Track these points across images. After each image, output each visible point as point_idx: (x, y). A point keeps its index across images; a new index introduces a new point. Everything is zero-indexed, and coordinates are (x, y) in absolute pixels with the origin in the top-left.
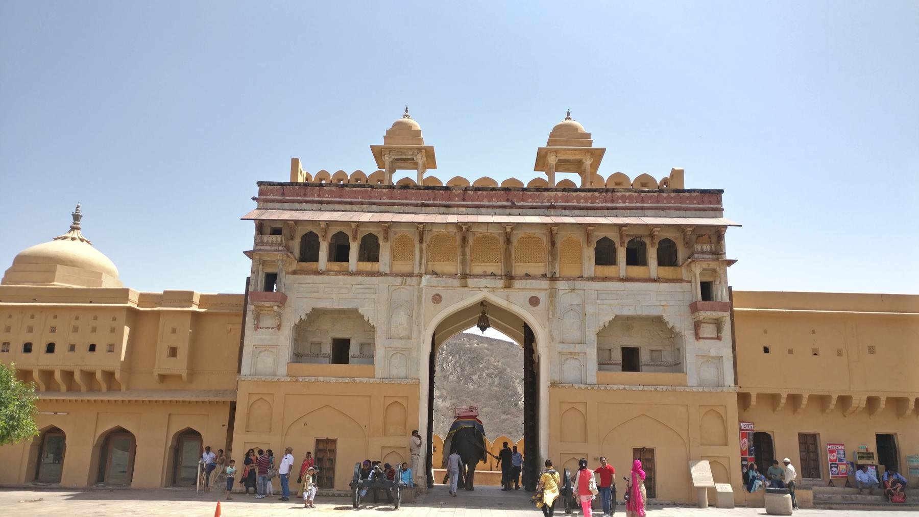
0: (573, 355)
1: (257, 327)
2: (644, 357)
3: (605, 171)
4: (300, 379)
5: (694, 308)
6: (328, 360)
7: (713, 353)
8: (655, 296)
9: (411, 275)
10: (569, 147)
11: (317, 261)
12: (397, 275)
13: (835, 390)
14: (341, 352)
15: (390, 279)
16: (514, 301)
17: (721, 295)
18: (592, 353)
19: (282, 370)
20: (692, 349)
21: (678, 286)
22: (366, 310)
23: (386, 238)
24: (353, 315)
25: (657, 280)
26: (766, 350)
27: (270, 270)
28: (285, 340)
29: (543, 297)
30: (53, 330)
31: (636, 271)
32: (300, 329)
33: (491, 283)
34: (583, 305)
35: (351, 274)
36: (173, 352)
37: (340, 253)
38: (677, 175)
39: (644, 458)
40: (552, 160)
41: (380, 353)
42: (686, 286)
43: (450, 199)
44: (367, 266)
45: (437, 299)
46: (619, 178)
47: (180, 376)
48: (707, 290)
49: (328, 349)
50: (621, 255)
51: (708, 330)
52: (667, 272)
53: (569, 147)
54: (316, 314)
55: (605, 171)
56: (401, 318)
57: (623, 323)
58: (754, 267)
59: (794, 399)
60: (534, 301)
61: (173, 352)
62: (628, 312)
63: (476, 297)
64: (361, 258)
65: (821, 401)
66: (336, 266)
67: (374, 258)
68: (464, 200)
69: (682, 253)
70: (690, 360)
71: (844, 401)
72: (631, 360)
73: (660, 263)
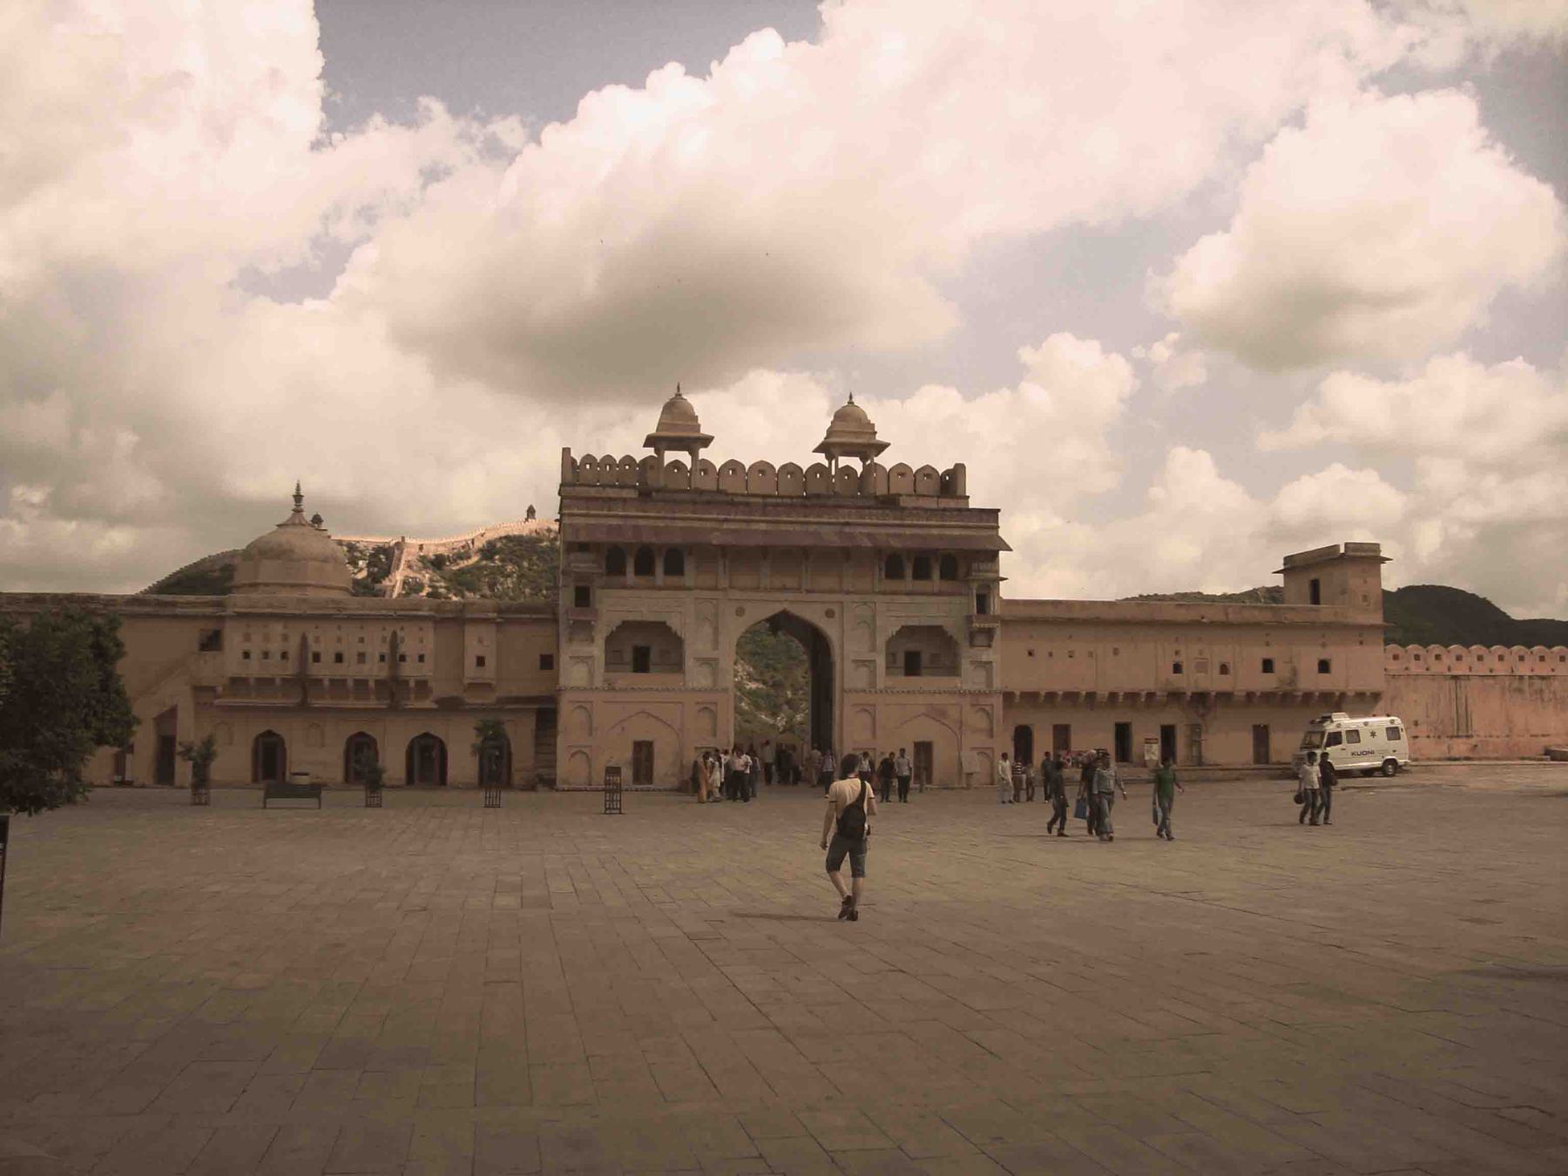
0: (862, 663)
1: (570, 640)
2: (925, 659)
3: (886, 460)
4: (617, 686)
5: (969, 619)
6: (630, 667)
7: (984, 658)
8: (937, 607)
9: (715, 589)
10: (851, 434)
11: (624, 573)
12: (702, 589)
13: (1083, 689)
14: (641, 663)
15: (697, 593)
16: (812, 613)
17: (995, 609)
18: (881, 661)
19: (599, 682)
20: (967, 656)
21: (956, 599)
22: (674, 623)
23: (690, 554)
24: (661, 628)
25: (940, 594)
26: (1030, 654)
27: (581, 584)
28: (597, 650)
29: (836, 609)
30: (362, 640)
31: (922, 585)
32: (610, 640)
33: (790, 596)
34: (874, 617)
35: (660, 589)
36: (481, 661)
37: (645, 567)
38: (958, 471)
39: (924, 750)
40: (834, 451)
41: (689, 663)
42: (964, 600)
43: (750, 514)
44: (674, 580)
45: (740, 612)
46: (902, 470)
47: (489, 685)
48: (983, 603)
49: (629, 656)
50: (909, 572)
51: (980, 639)
52: (947, 586)
53: (851, 434)
54: (626, 626)
55: (886, 460)
56: (707, 630)
57: (907, 632)
58: (1022, 578)
59: (1051, 696)
60: (830, 614)
61: (481, 661)
62: (911, 623)
63: (777, 608)
64: (667, 572)
65: (1071, 696)
66: (642, 580)
67: (681, 572)
68: (764, 514)
69: (962, 571)
70: (965, 665)
71: (1091, 696)
72: (912, 665)
73: (942, 577)
